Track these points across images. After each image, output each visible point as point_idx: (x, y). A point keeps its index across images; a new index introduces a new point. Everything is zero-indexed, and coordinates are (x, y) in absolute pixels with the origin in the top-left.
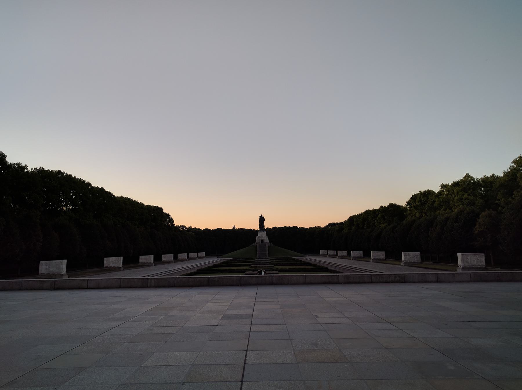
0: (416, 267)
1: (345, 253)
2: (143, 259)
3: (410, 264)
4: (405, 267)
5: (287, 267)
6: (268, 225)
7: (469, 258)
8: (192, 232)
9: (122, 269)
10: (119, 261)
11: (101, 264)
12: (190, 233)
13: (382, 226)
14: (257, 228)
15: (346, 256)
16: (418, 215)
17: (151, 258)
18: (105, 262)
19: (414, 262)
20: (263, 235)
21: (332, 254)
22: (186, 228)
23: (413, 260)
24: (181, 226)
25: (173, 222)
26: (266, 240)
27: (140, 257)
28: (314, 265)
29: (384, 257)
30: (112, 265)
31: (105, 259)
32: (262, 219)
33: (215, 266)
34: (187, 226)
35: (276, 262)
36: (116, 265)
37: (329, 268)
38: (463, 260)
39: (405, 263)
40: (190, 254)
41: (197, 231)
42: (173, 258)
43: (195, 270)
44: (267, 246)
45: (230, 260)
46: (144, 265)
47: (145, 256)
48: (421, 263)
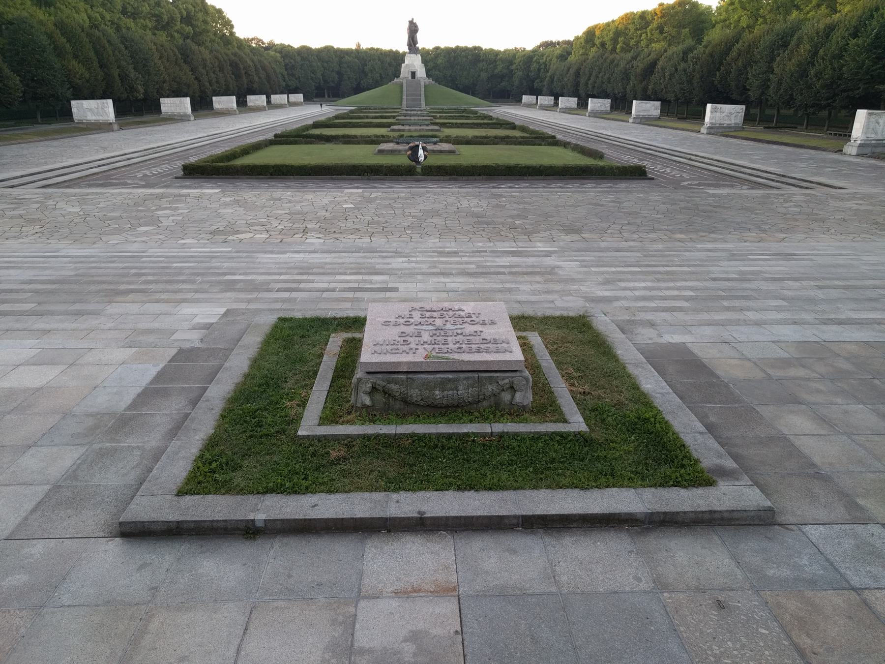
0: (735, 137)
1: (573, 102)
2: (168, 105)
3: (718, 131)
4: (709, 137)
5: (470, 133)
6: (425, 42)
7: (881, 121)
8: (276, 51)
9: (116, 127)
10: (105, 110)
11: (67, 114)
12: (272, 53)
13: (656, 46)
15: (574, 109)
16: (744, 22)
17: (184, 104)
18: (74, 110)
20: (414, 63)
21: (546, 103)
22: (263, 43)
23: (726, 122)
24: (253, 39)
25: (232, 27)
26: (421, 73)
27: (162, 100)
28: (523, 129)
30: (91, 117)
31: (73, 103)
32: (413, 29)
33: (317, 125)
34: (266, 40)
35: (441, 117)
36: (101, 119)
37: (559, 137)
38: (867, 128)
39: (709, 128)
40: (272, 96)
41: (285, 52)
42: (235, 105)
43: (270, 136)
44: (422, 84)
45: (352, 112)
47: (171, 99)
48: (743, 129)
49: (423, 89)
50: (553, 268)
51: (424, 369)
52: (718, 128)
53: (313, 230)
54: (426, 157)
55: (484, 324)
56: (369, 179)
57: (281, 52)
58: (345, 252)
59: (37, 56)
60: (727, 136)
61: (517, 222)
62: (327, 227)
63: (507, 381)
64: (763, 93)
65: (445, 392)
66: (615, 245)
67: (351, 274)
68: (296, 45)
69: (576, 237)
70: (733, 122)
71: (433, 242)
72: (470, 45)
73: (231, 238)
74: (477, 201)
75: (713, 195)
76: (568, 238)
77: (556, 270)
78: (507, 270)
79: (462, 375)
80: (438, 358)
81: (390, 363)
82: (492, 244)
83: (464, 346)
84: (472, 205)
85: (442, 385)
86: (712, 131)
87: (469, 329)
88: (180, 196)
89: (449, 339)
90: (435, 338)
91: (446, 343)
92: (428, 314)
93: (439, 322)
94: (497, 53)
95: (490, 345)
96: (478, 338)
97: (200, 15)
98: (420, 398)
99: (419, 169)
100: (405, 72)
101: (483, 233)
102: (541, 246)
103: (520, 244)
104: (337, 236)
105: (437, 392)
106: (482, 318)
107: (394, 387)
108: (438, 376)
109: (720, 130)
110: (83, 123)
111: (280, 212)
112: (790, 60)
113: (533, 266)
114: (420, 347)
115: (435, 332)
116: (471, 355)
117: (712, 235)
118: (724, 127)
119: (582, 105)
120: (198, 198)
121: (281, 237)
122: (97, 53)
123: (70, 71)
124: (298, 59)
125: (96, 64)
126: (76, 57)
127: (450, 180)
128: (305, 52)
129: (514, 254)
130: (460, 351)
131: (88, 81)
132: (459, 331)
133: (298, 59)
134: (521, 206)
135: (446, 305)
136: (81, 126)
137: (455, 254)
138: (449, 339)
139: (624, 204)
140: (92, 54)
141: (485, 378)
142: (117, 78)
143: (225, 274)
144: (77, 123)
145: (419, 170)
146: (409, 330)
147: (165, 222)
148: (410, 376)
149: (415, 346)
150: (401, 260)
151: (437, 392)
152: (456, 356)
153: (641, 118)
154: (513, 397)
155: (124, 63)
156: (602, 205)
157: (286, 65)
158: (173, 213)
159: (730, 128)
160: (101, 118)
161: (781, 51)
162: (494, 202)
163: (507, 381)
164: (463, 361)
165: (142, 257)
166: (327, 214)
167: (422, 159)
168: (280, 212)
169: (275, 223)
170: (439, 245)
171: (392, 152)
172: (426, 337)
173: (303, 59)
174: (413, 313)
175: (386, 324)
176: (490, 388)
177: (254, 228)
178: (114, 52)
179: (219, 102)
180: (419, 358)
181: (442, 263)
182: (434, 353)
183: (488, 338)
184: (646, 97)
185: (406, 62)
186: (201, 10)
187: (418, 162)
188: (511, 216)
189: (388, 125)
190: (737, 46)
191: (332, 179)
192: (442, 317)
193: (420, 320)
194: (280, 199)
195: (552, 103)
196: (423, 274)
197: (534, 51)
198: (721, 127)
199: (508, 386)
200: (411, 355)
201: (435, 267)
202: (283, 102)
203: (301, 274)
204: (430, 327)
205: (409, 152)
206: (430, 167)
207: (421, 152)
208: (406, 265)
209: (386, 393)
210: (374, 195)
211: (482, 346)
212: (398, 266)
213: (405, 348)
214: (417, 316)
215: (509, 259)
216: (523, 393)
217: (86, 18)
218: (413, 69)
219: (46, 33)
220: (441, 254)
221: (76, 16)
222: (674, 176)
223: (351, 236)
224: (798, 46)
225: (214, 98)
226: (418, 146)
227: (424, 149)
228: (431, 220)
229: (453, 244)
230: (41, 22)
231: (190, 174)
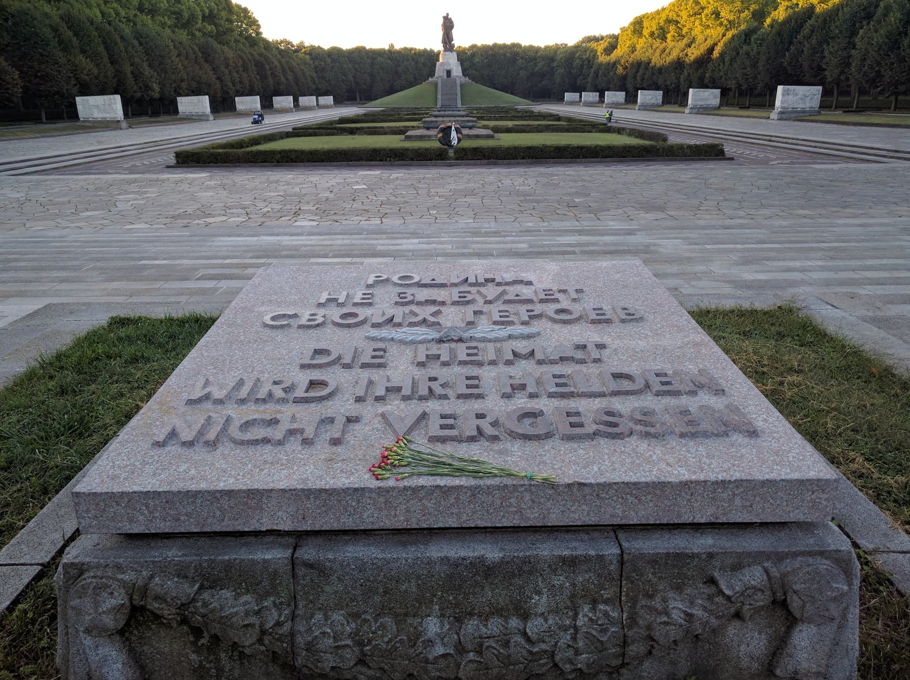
1: (620, 96)
2: (185, 104)
5: (510, 124)
6: (462, 40)
12: (301, 55)
14: (437, 46)
15: (622, 104)
18: (79, 107)
19: (803, 111)
20: (450, 62)
21: (591, 99)
22: (293, 46)
23: (800, 106)
24: (282, 42)
25: (259, 26)
26: (457, 71)
29: (716, 101)
30: (98, 115)
31: (78, 99)
32: (448, 25)
36: (109, 116)
39: (781, 113)
41: (315, 54)
42: (259, 106)
44: (458, 82)
46: (190, 119)
49: (459, 88)
50: (648, 246)
51: (370, 518)
52: (791, 112)
53: (309, 211)
54: (459, 140)
55: (601, 320)
56: (392, 165)
57: (310, 54)
58: (341, 234)
59: (40, 50)
60: (802, 121)
61: (577, 200)
62: (324, 210)
63: (754, 576)
64: (842, 72)
65: (471, 626)
66: (720, 223)
67: (334, 257)
68: (326, 46)
69: (660, 215)
70: (808, 105)
71: (466, 221)
72: (508, 42)
73: (197, 221)
74: (521, 180)
75: (821, 170)
76: (650, 216)
77: (652, 248)
78: (577, 249)
79: (547, 550)
80: (437, 466)
81: (216, 496)
82: (546, 224)
83: (543, 404)
84: (516, 183)
85: (458, 589)
86: (784, 116)
87: (556, 338)
88: (158, 180)
89: (487, 374)
90: (434, 370)
91: (473, 391)
92: (423, 294)
93: (452, 318)
94: (537, 50)
95: (647, 401)
96: (592, 370)
97: (224, 14)
98: (351, 656)
99: (451, 153)
100: (439, 71)
101: (534, 212)
102: (614, 225)
103: (585, 223)
104: (335, 217)
105: (433, 626)
106: (589, 304)
107: (231, 604)
108: (437, 551)
109: (793, 115)
110: (89, 122)
111: (272, 194)
112: (876, 31)
113: (615, 244)
114: (369, 411)
115: (434, 350)
116: (582, 450)
117: (848, 210)
118: (797, 112)
119: (631, 99)
120: (176, 183)
121: (262, 220)
122: (107, 48)
123: (76, 66)
124: (329, 60)
125: (106, 59)
126: (83, 52)
127: (488, 164)
128: (335, 54)
129: (580, 232)
130: (531, 430)
131: (96, 78)
132: (522, 346)
133: (329, 60)
134: (579, 184)
135: (477, 268)
136: (88, 124)
137: (496, 233)
138: (487, 374)
139: (711, 181)
140: (101, 49)
141: (654, 561)
142: (130, 75)
143: (141, 259)
144: (83, 121)
145: (451, 153)
146: (354, 341)
147: (121, 206)
148: (308, 552)
149: (350, 408)
150: (417, 241)
151: (433, 626)
152: (518, 460)
153: (699, 108)
154: (779, 646)
155: (137, 60)
156: (683, 182)
157: (316, 68)
158: (138, 197)
159: (804, 112)
160: (108, 115)
161: (865, 23)
162: (544, 180)
163: (754, 576)
164: (548, 484)
165: (51, 242)
166: (331, 196)
167: (455, 142)
168: (272, 194)
169: (261, 205)
170: (475, 225)
171: (421, 138)
172: (401, 369)
173: (333, 61)
174: (378, 291)
175: (282, 323)
176: (677, 606)
177: (231, 211)
178: (126, 48)
179: (242, 103)
180: (351, 472)
181: (478, 243)
182: (420, 443)
183: (633, 369)
184: (703, 85)
185: (441, 60)
186: (224, 9)
187: (451, 146)
188: (570, 194)
189: (419, 120)
190: (810, 22)
191: (349, 166)
192: (462, 302)
193: (390, 312)
194: (277, 182)
195: (597, 99)
196: (446, 255)
197: (577, 47)
198: (795, 111)
199: (762, 600)
200: (322, 450)
201: (465, 248)
202: (311, 104)
203: (258, 257)
204: (422, 333)
205: (440, 135)
206: (464, 150)
207: (454, 134)
208: (425, 246)
209: (194, 626)
210: (394, 176)
211: (619, 405)
212: (411, 247)
213: (308, 416)
214: (385, 303)
215: (573, 238)
216: (829, 630)
217: (98, 14)
218: (448, 68)
219: (51, 26)
220: (476, 234)
221: (87, 11)
222: (756, 156)
223: (355, 218)
224: (885, 15)
225: (237, 99)
226: (450, 127)
227: (457, 130)
228: (465, 200)
229: (493, 224)
230: (46, 15)
231: (184, 162)
